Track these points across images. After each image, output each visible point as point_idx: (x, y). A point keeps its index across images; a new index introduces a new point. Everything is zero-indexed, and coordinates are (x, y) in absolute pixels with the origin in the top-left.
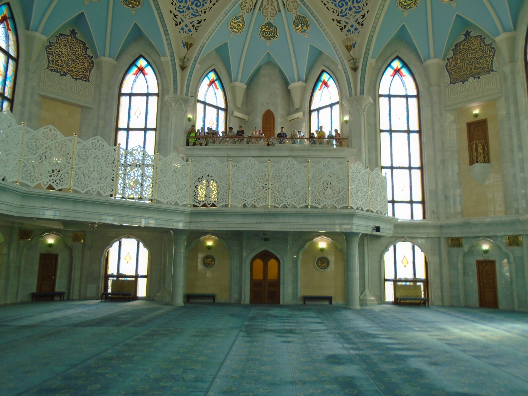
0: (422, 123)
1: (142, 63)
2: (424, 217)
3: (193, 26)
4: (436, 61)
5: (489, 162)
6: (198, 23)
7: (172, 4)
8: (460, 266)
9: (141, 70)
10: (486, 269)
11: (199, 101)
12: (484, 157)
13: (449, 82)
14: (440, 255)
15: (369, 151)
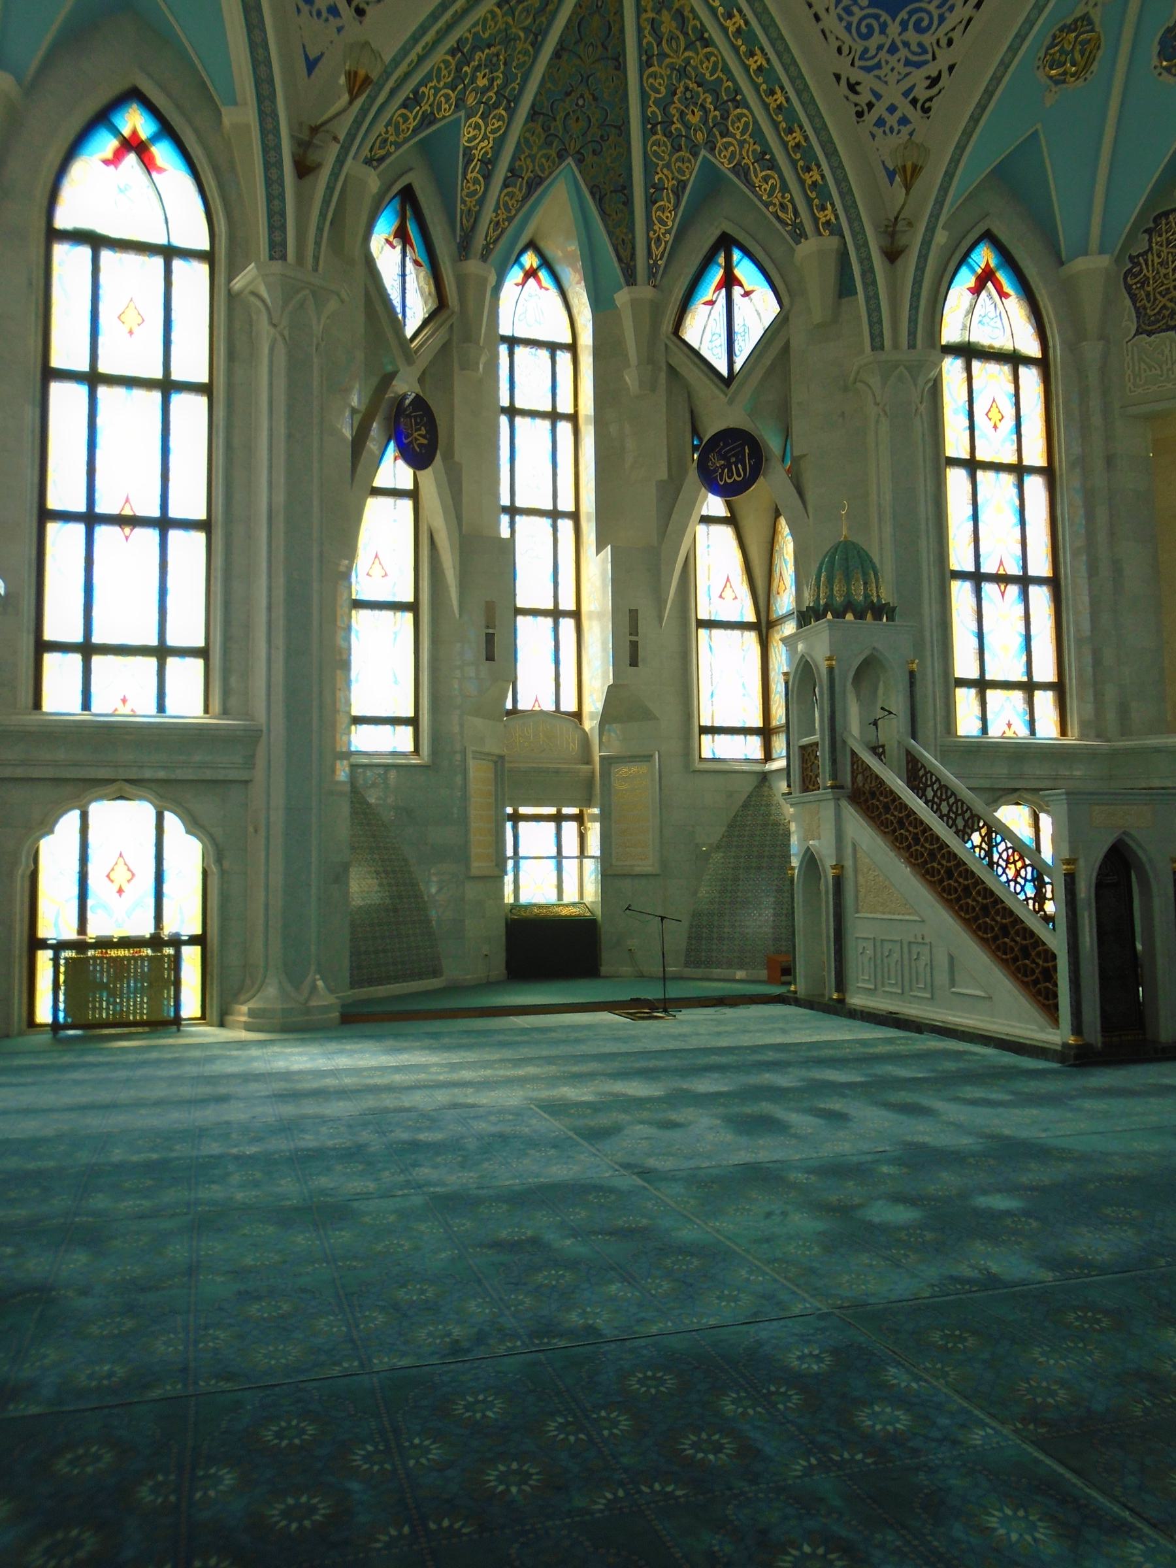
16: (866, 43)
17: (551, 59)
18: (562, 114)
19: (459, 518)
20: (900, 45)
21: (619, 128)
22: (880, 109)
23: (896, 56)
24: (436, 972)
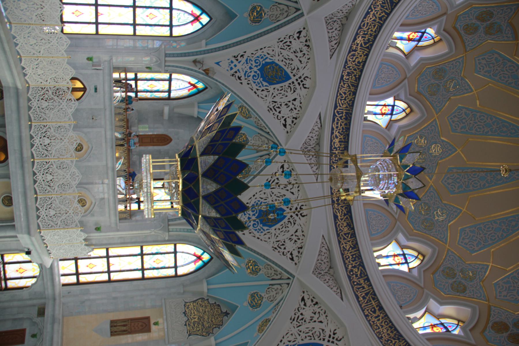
1: (205, 19)
2: (64, 285)
3: (236, 72)
4: (206, 290)
5: (112, 335)
6: (238, 77)
7: (252, 54)
9: (197, 19)
11: (171, 75)
12: (115, 332)
14: (30, 299)
15: (121, 238)
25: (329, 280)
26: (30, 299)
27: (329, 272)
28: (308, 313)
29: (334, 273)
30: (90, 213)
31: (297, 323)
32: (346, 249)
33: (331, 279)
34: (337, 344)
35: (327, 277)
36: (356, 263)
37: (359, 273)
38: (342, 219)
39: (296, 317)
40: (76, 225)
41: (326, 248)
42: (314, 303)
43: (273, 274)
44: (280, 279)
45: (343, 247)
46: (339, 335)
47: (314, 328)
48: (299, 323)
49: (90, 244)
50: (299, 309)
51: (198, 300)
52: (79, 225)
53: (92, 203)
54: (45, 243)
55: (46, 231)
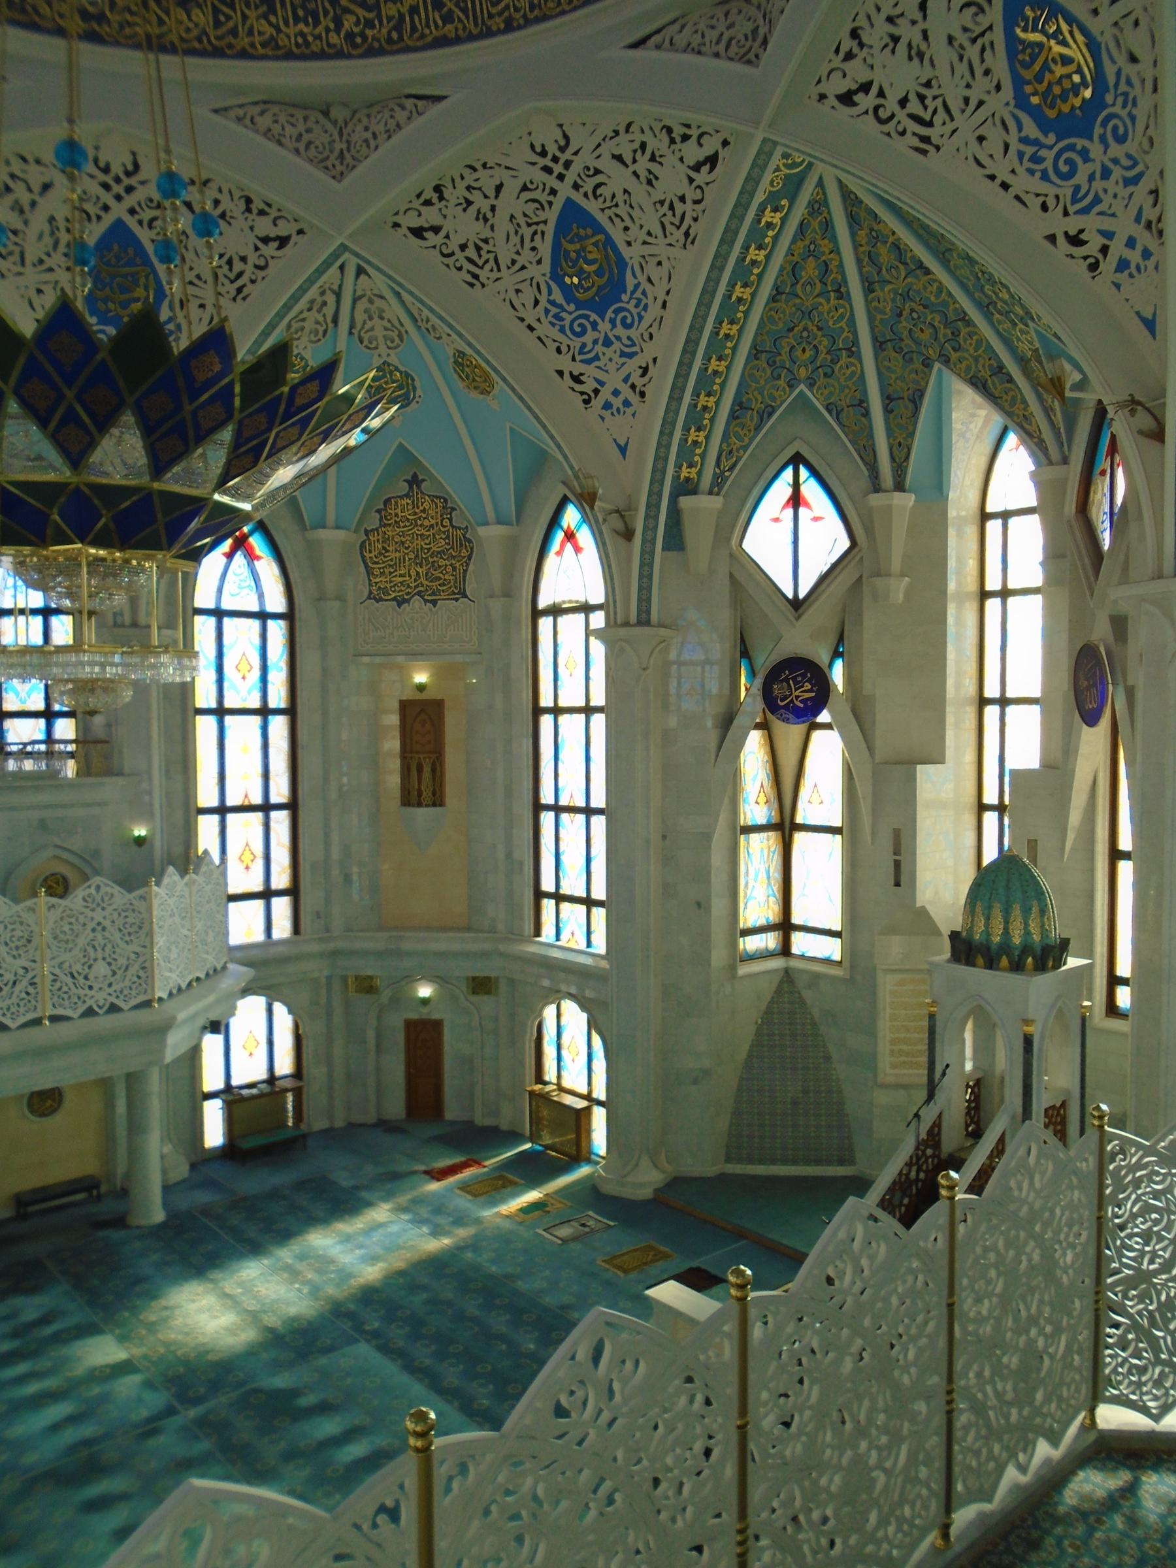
0: (299, 692)
2: (296, 928)
4: (341, 534)
5: (442, 804)
8: (371, 1034)
10: (423, 1037)
12: (434, 794)
13: (366, 594)
14: (329, 1014)
15: (167, 771)
16: (1074, 181)
17: (866, 297)
18: (906, 333)
19: (870, 748)
20: (1110, 165)
21: (963, 319)
22: (1117, 249)
23: (1113, 178)
24: (841, 1162)
25: (366, 129)
26: (329, 1014)
27: (341, 122)
28: (463, 228)
29: (345, 105)
30: (90, 864)
31: (488, 267)
32: (272, 38)
33: (365, 121)
34: (576, 153)
35: (359, 135)
36: (326, 13)
37: (361, 12)
38: (161, 22)
39: (467, 266)
40: (142, 898)
41: (256, 110)
42: (435, 200)
43: (321, 319)
44: (338, 295)
45: (264, 45)
46: (549, 138)
47: (512, 217)
48: (487, 261)
49: (186, 857)
50: (445, 251)
51: (364, 562)
52: (141, 892)
53: (56, 857)
54: (190, 985)
55: (157, 984)
